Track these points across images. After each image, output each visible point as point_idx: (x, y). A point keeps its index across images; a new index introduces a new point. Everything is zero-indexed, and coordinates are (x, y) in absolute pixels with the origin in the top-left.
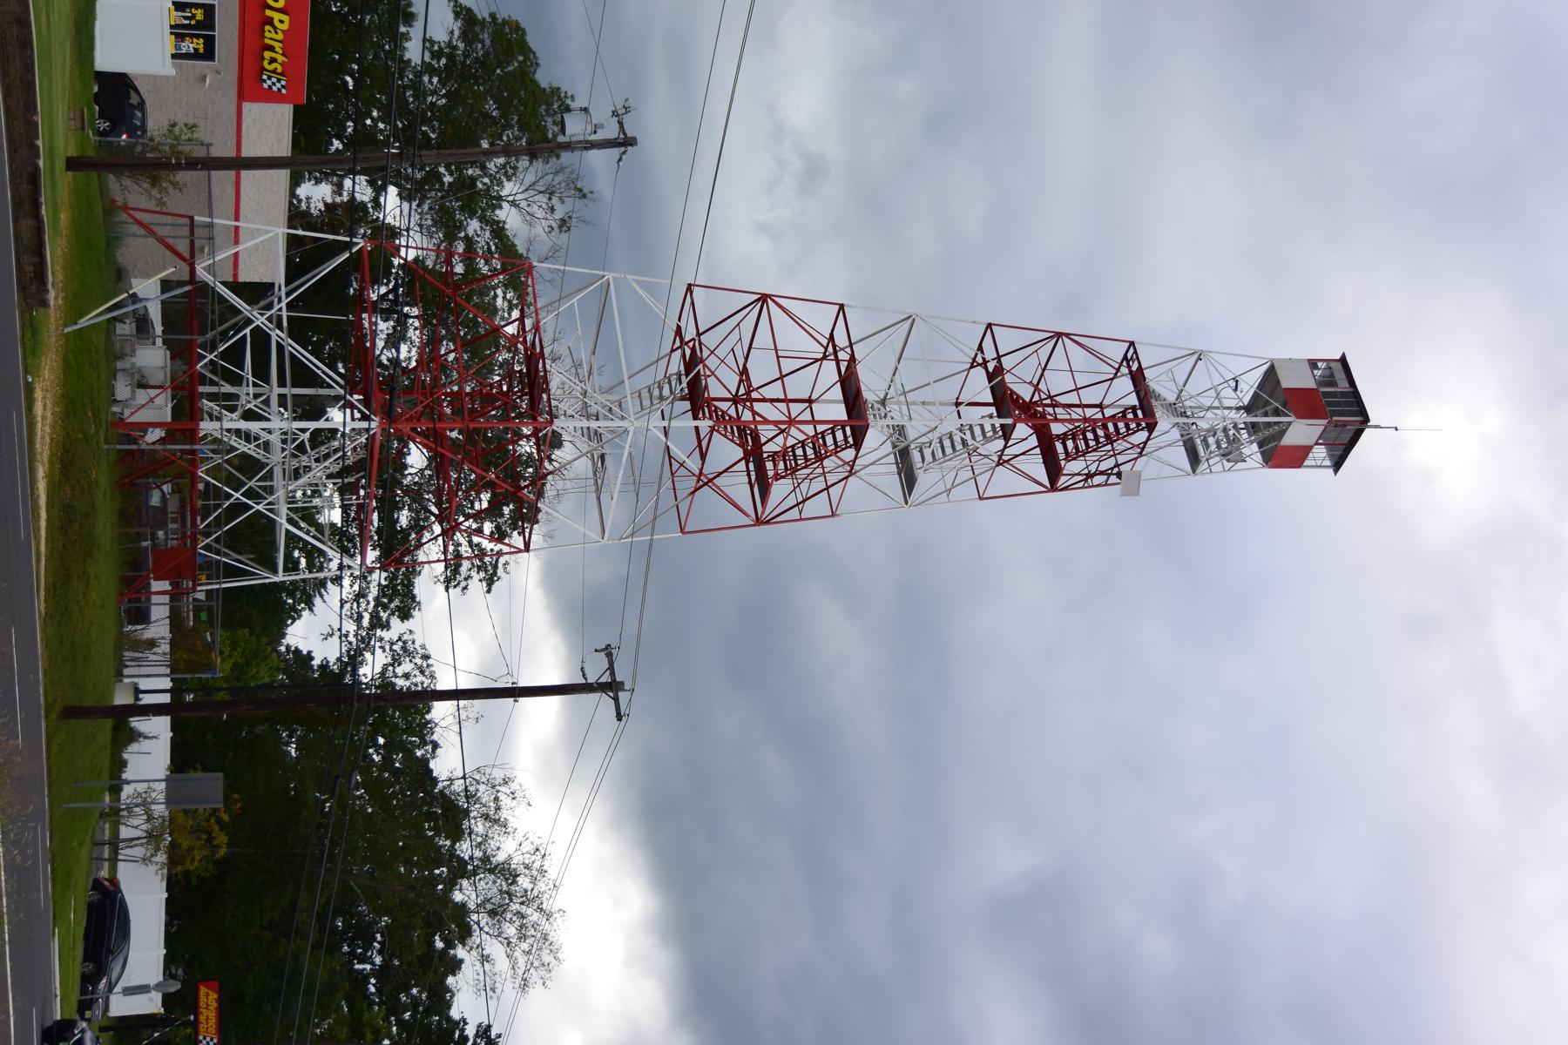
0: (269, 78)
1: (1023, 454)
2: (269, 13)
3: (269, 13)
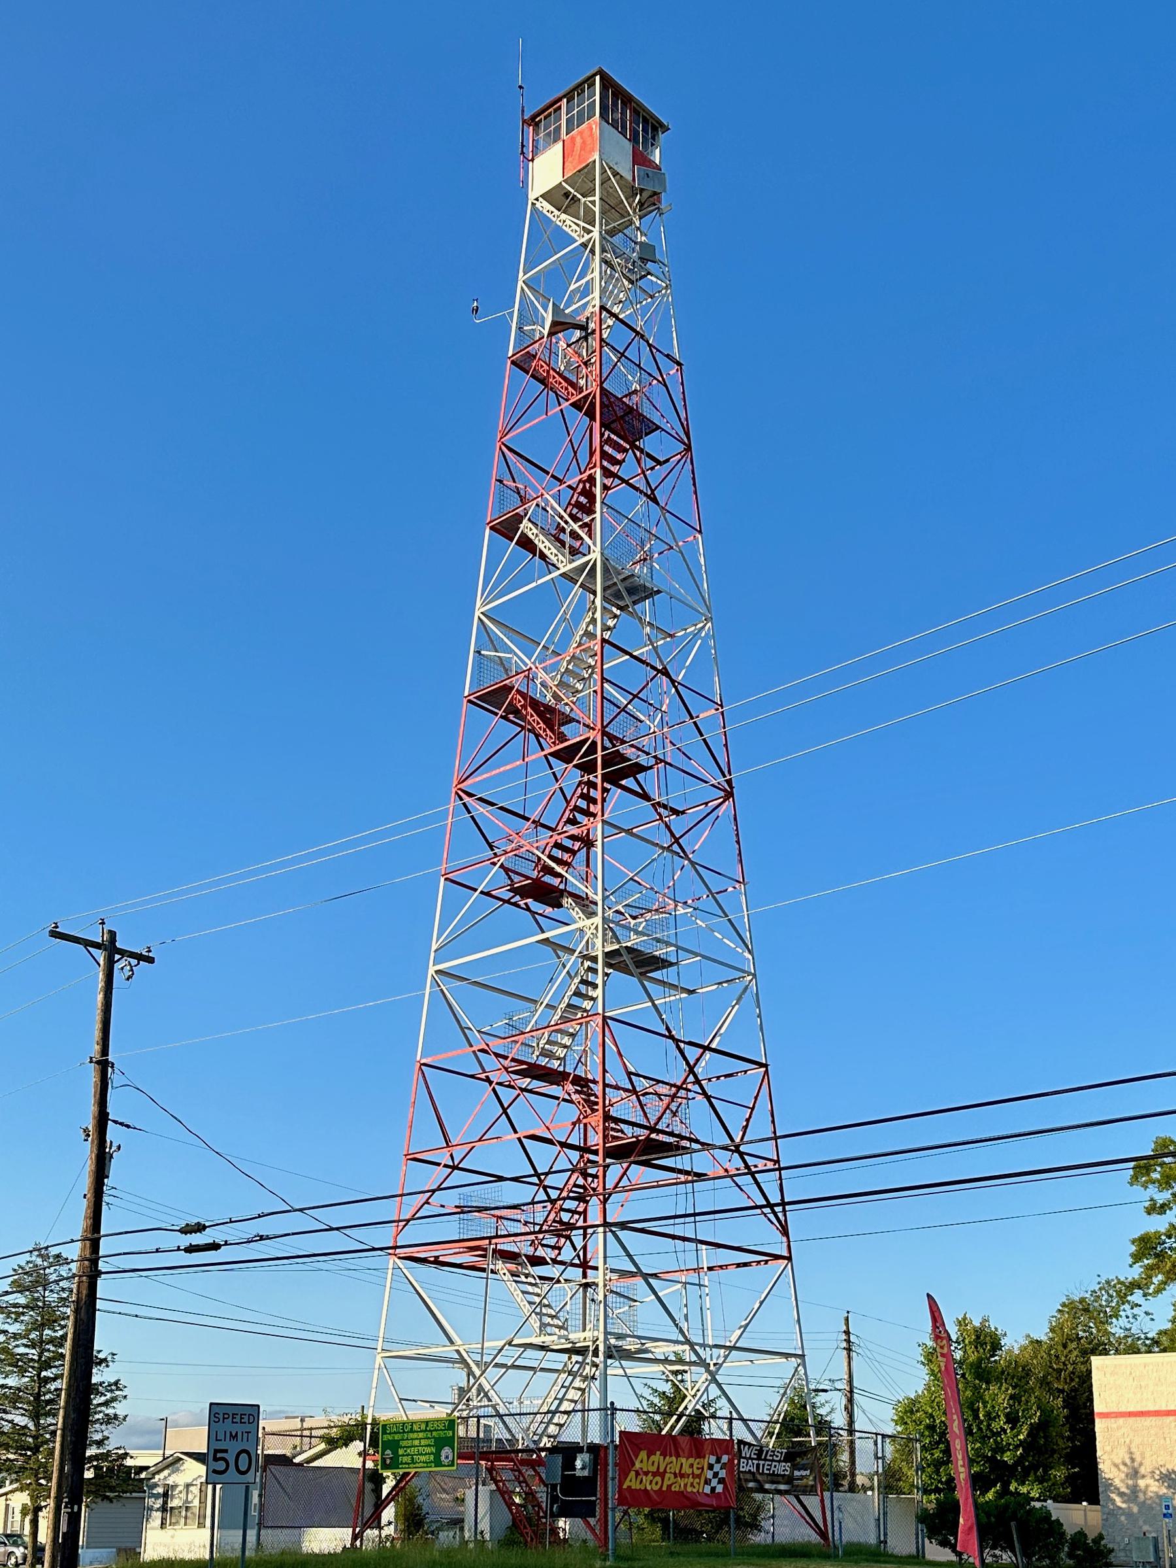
0: (708, 1482)
1: (301, 1210)
2: (664, 1488)
3: (664, 1488)
